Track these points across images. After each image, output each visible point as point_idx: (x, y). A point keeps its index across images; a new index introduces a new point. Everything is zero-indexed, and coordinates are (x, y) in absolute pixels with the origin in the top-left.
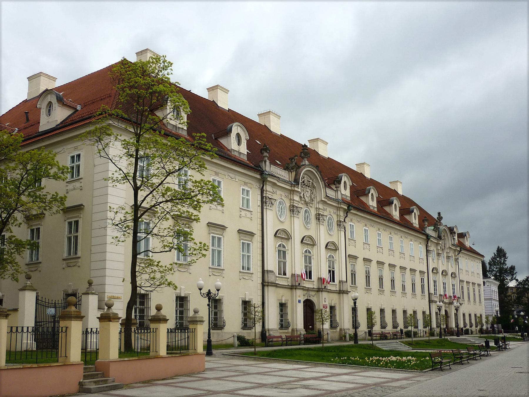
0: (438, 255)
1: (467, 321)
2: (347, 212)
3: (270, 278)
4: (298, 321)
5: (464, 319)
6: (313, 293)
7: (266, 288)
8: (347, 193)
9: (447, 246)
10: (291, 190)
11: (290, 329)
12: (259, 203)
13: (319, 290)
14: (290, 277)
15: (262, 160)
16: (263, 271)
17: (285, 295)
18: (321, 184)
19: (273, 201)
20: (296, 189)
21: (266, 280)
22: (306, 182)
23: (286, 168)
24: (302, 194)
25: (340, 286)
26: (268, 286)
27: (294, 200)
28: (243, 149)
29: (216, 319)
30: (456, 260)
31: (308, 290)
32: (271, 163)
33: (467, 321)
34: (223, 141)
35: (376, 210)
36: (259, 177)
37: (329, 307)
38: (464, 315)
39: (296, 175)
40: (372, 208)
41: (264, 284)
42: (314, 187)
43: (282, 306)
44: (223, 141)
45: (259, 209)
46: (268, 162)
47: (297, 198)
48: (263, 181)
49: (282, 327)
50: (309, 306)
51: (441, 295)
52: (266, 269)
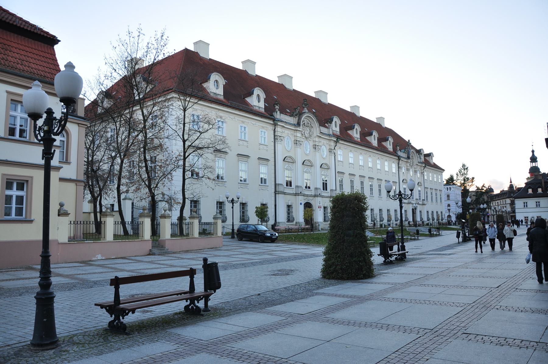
0: (408, 170)
1: (430, 217)
2: (336, 142)
3: (280, 189)
4: (299, 216)
5: (428, 215)
6: (311, 198)
7: (277, 195)
8: (338, 129)
9: (415, 164)
11: (294, 223)
12: (273, 140)
13: (315, 196)
15: (274, 110)
17: (291, 200)
18: (317, 124)
19: (282, 138)
20: (298, 129)
21: (277, 190)
28: (262, 105)
29: (243, 216)
30: (422, 173)
31: (307, 196)
32: (281, 113)
33: (430, 217)
34: (248, 100)
35: (359, 140)
36: (272, 122)
37: (322, 208)
38: (428, 212)
39: (299, 120)
40: (356, 139)
41: (276, 192)
42: (312, 127)
43: (289, 207)
44: (248, 100)
46: (278, 112)
47: (299, 135)
48: (275, 125)
49: (289, 220)
50: (308, 206)
51: (417, 199)
52: (277, 183)
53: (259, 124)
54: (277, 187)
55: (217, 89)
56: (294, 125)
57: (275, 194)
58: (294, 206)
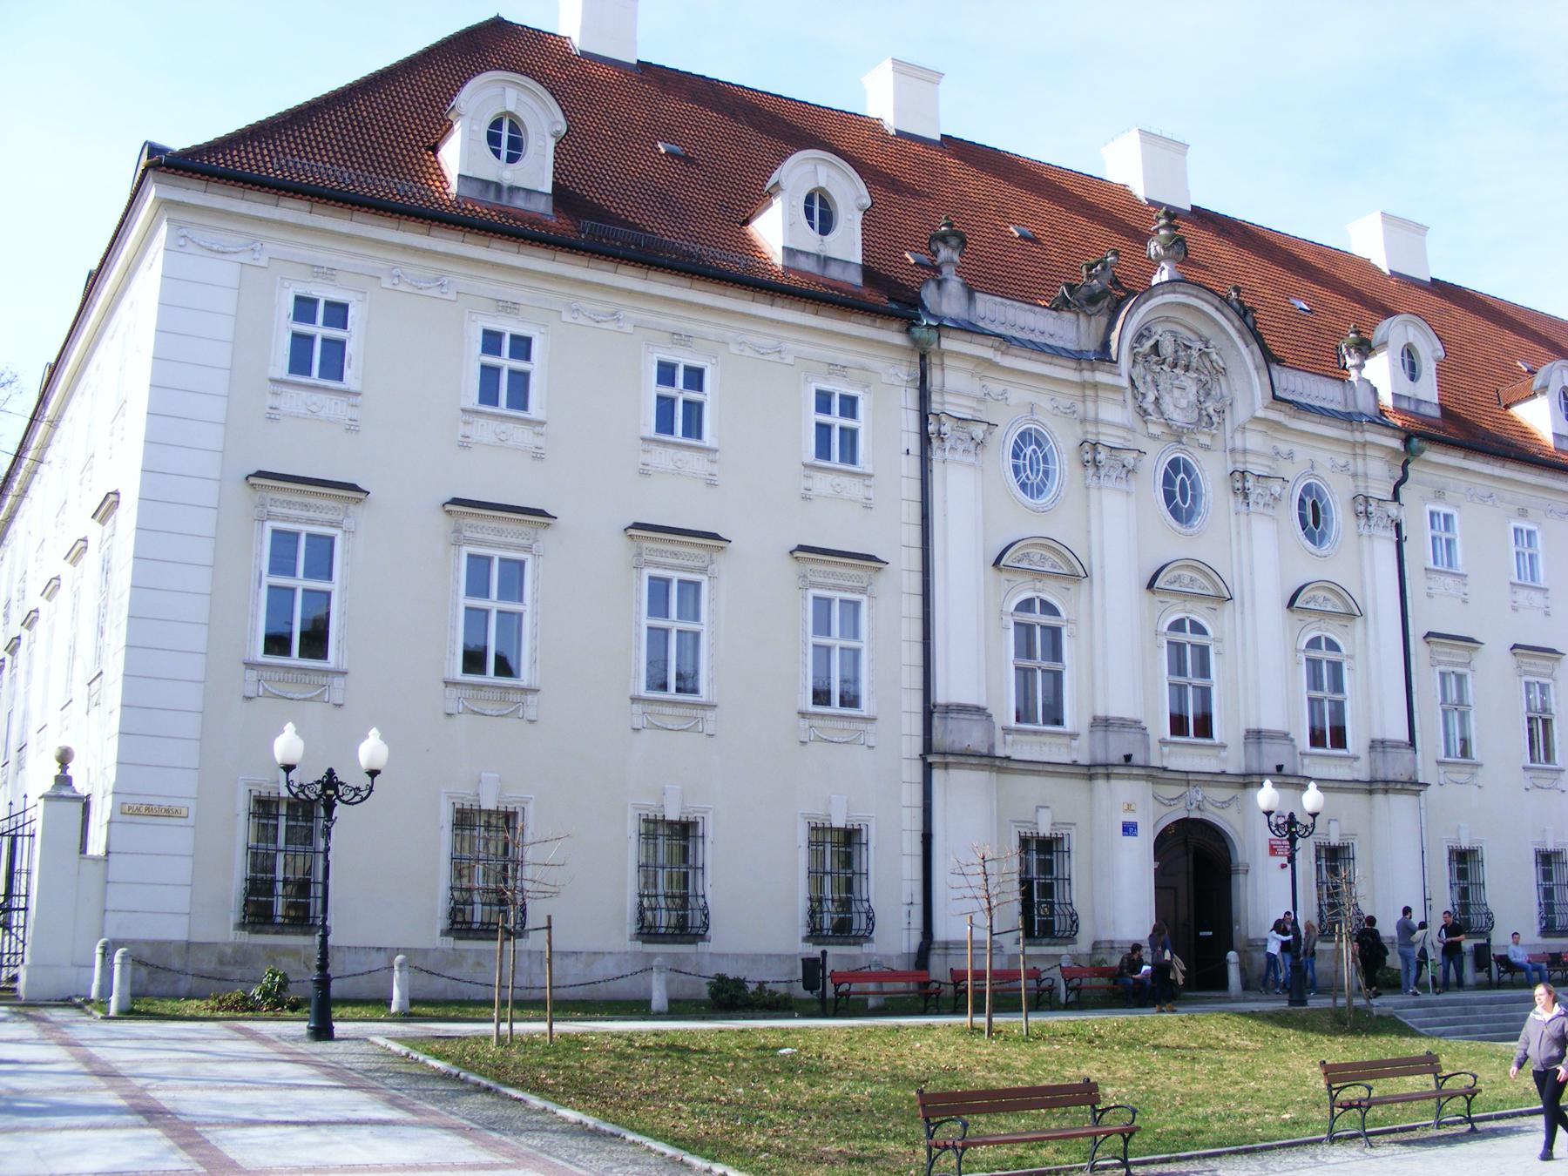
6: (1221, 794)
7: (937, 775)
10: (1083, 385)
12: (913, 443)
14: (1084, 729)
16: (929, 711)
22: (1167, 349)
23: (1061, 305)
24: (1151, 397)
25: (1372, 762)
26: (946, 766)
27: (1096, 421)
31: (1187, 778)
41: (932, 757)
45: (912, 466)
52: (941, 696)
53: (807, 350)
54: (936, 721)
55: (512, 159)
56: (1077, 357)
57: (928, 769)
58: (1077, 845)
